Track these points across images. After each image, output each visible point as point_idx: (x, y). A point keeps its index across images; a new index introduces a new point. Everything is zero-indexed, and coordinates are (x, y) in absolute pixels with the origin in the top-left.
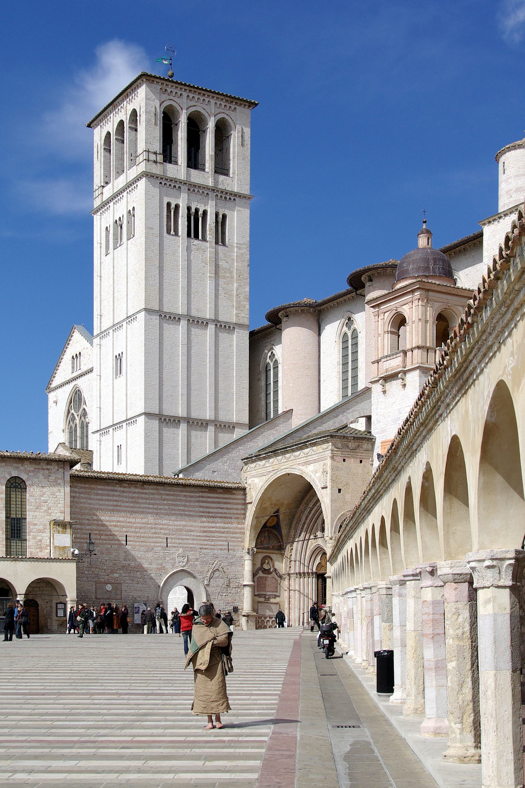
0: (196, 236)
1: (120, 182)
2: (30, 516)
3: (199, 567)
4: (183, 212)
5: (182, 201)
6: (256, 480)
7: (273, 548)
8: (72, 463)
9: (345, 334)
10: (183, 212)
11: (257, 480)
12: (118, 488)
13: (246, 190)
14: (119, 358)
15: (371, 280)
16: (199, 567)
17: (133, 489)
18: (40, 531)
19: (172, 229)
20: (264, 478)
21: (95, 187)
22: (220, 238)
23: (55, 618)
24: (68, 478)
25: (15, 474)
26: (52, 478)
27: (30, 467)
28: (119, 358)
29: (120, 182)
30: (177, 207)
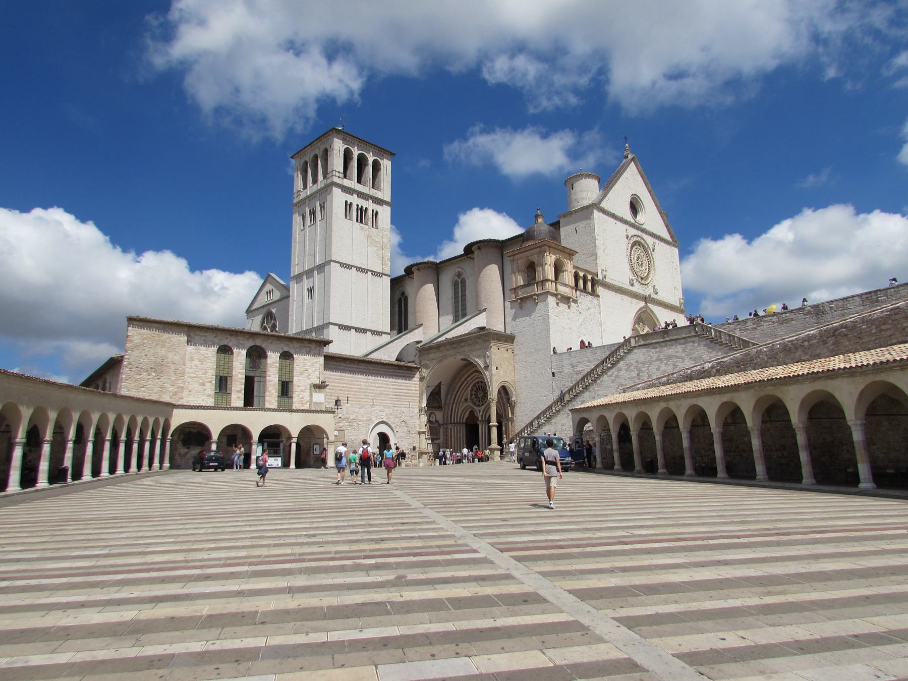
2: (296, 380)
3: (392, 420)
4: (354, 207)
5: (355, 200)
7: (436, 407)
10: (354, 207)
12: (343, 364)
13: (388, 199)
15: (479, 248)
16: (392, 420)
17: (352, 365)
18: (302, 391)
21: (295, 191)
23: (312, 455)
25: (286, 349)
27: (297, 345)
30: (351, 204)
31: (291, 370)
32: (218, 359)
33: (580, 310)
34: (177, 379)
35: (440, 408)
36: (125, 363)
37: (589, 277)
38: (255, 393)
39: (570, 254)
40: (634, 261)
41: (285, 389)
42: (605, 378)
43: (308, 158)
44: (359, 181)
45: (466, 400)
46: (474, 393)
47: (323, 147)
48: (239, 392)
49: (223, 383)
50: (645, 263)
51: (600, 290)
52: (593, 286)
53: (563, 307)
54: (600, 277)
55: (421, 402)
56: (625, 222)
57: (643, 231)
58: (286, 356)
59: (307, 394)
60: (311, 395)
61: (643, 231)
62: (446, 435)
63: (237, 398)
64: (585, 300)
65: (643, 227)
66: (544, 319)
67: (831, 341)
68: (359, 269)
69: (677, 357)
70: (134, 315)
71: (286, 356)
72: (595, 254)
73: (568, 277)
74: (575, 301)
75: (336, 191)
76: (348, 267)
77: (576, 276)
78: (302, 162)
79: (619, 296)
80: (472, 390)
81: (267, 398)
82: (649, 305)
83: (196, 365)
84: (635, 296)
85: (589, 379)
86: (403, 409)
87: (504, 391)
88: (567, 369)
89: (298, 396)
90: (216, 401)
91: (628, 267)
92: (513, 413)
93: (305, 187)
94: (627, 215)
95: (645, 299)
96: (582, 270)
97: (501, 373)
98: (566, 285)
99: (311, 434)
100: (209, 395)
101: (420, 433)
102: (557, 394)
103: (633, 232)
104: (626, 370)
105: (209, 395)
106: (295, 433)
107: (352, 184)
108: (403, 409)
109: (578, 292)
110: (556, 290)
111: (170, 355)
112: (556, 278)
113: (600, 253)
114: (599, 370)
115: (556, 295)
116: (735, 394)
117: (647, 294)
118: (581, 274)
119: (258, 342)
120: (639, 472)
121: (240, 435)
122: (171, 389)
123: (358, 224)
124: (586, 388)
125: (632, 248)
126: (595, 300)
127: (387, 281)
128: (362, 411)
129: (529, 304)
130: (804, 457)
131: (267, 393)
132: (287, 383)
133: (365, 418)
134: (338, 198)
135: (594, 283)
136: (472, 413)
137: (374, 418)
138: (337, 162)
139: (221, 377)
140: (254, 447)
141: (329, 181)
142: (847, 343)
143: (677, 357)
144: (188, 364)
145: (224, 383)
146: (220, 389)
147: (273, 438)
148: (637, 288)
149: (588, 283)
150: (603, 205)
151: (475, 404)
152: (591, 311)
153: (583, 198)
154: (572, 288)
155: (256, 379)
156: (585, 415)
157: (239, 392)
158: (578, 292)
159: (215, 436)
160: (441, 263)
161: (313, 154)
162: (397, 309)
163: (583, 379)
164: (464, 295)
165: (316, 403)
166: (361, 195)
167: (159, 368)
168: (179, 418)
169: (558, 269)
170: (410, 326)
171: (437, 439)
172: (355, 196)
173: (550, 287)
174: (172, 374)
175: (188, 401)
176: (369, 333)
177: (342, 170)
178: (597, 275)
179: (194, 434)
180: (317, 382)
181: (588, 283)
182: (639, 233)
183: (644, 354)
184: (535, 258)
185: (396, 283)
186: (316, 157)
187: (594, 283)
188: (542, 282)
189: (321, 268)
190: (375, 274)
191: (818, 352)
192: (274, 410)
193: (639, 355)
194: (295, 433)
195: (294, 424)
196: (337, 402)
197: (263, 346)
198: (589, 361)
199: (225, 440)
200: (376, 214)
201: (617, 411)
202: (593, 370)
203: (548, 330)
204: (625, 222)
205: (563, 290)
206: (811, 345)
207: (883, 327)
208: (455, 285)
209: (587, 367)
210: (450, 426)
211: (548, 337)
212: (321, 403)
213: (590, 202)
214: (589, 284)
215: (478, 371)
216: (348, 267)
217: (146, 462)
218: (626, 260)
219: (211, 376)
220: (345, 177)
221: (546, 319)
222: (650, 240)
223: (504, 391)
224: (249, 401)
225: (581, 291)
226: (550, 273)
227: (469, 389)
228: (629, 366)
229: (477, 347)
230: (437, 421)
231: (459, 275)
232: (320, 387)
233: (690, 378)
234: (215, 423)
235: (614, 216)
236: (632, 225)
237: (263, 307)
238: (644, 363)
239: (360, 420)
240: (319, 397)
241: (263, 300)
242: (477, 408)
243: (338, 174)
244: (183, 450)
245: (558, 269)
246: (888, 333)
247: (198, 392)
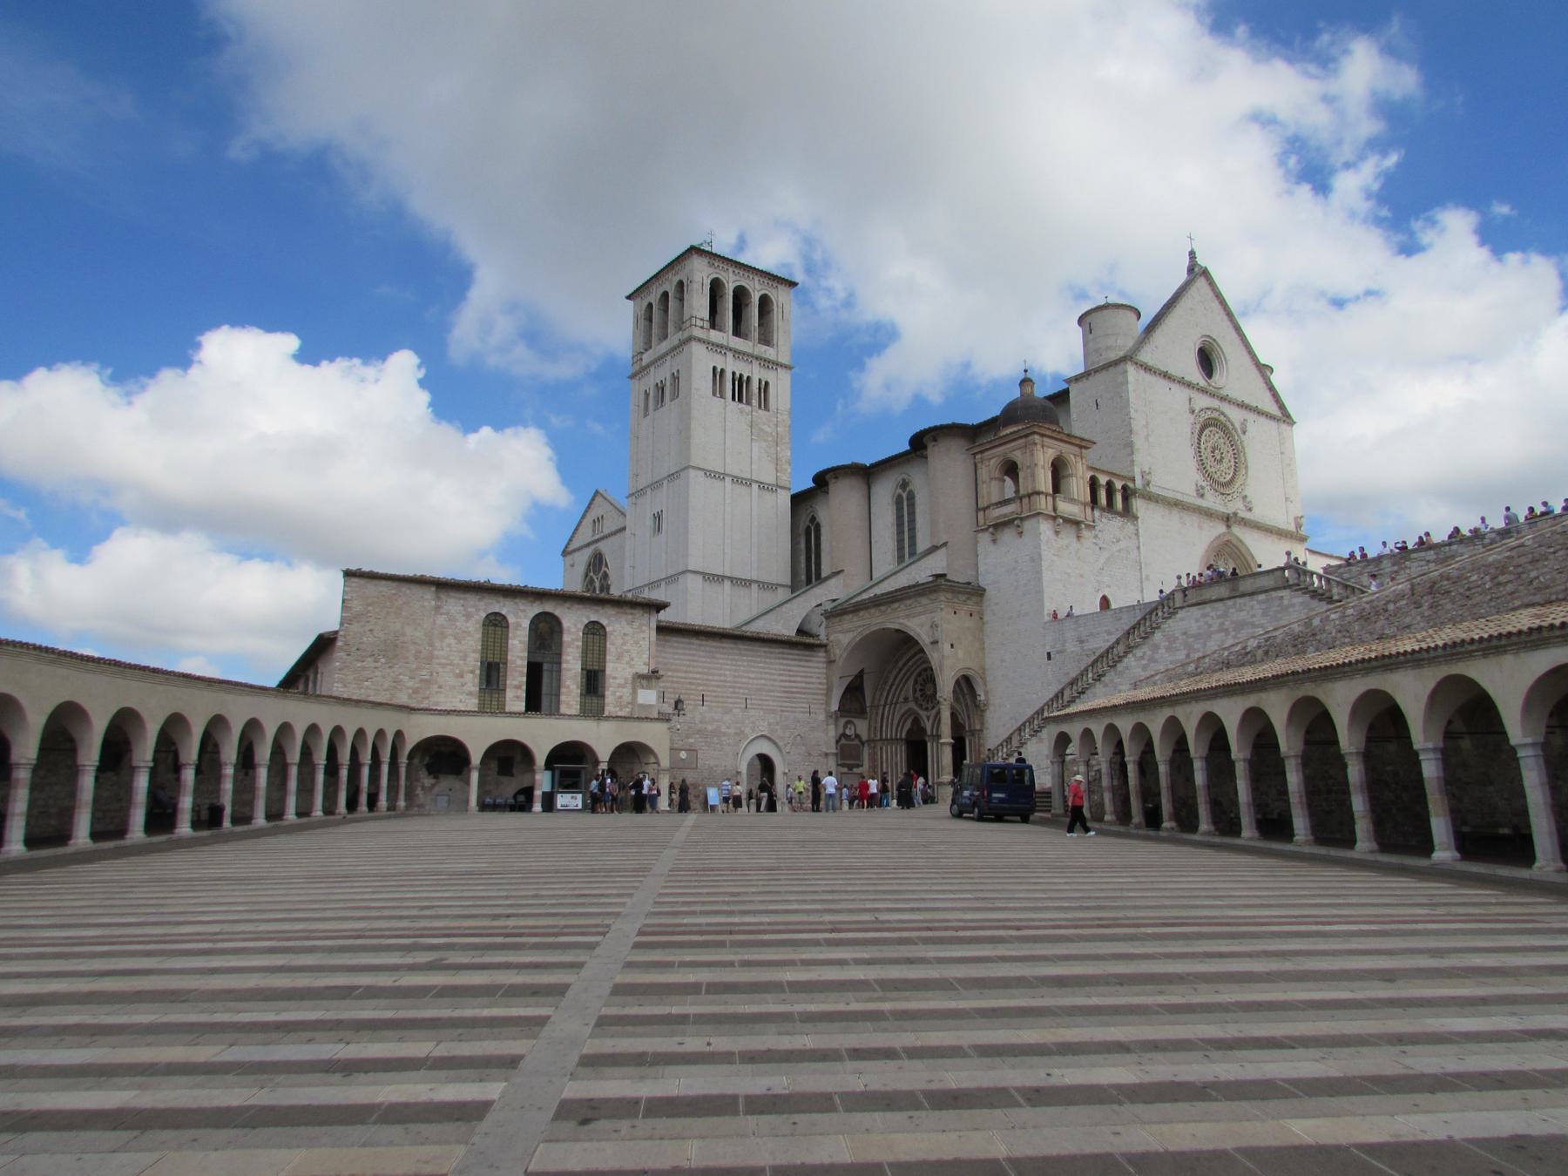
0: (740, 400)
1: (665, 346)
2: (610, 668)
4: (729, 377)
6: (841, 636)
8: (659, 607)
9: (900, 496)
10: (729, 377)
11: (844, 637)
14: (658, 518)
19: (718, 390)
20: (851, 635)
22: (764, 403)
24: (653, 625)
25: (594, 618)
26: (636, 625)
27: (611, 611)
28: (658, 518)
29: (665, 346)
30: (722, 371)
31: (603, 652)
32: (485, 635)
33: (1100, 543)
34: (419, 669)
35: (862, 713)
36: (339, 643)
37: (1118, 485)
38: (545, 689)
39: (1083, 444)
40: (1206, 454)
41: (593, 682)
42: (1130, 660)
43: (654, 297)
44: (737, 332)
45: (906, 700)
46: (918, 687)
47: (676, 280)
48: (518, 687)
49: (492, 674)
50: (1229, 456)
51: (1138, 505)
52: (1126, 499)
53: (1068, 535)
54: (1139, 483)
55: (828, 703)
56: (1189, 385)
57: (1223, 399)
58: (595, 631)
59: (626, 692)
60: (634, 693)
61: (1223, 399)
62: (873, 758)
63: (515, 697)
64: (1110, 526)
65: (1224, 392)
66: (1032, 560)
67: (1426, 602)
68: (737, 480)
69: (1253, 625)
70: (354, 567)
71: (595, 631)
72: (1130, 445)
73: (1078, 486)
74: (1089, 527)
75: (697, 350)
76: (719, 476)
77: (1093, 483)
78: (645, 304)
79: (1176, 516)
80: (916, 682)
81: (563, 698)
82: (1236, 530)
83: (449, 645)
84: (1208, 514)
85: (1107, 660)
86: (799, 716)
87: (965, 685)
88: (1072, 647)
89: (614, 693)
90: (482, 704)
91: (1192, 464)
92: (982, 724)
93: (648, 346)
94: (1195, 374)
95: (1228, 520)
96: (1103, 472)
97: (961, 653)
98: (1072, 501)
99: (630, 753)
100: (470, 694)
101: (826, 755)
102: (1055, 689)
103: (1202, 401)
104: (1168, 649)
105: (470, 694)
106: (604, 754)
107: (725, 337)
108: (799, 716)
109: (1097, 513)
110: (1055, 509)
111: (408, 630)
112: (1056, 488)
113: (1138, 442)
114: (1121, 649)
115: (1054, 518)
116: (1263, 695)
117: (1229, 510)
118: (1103, 480)
119: (549, 607)
120: (1138, 827)
121: (518, 758)
122: (410, 684)
123: (736, 404)
124: (1099, 678)
125: (1202, 431)
126: (1130, 527)
127: (784, 500)
128: (727, 718)
129: (1008, 535)
130: (1359, 803)
131: (563, 690)
132: (596, 672)
133: (731, 731)
134: (701, 362)
135: (1127, 494)
136: (917, 721)
137: (747, 731)
138: (699, 304)
139: (490, 665)
140: (538, 777)
141: (686, 335)
142: (1449, 606)
143: (1253, 625)
144: (438, 644)
145: (494, 674)
146: (488, 682)
147: (570, 761)
148: (1212, 501)
149: (1116, 497)
150: (1145, 356)
151: (921, 706)
152: (1122, 544)
153: (1108, 348)
154: (1085, 505)
155: (545, 666)
156: (1065, 728)
157: (518, 687)
158: (1097, 513)
159: (476, 758)
160: (874, 466)
161: (661, 291)
162: (803, 545)
163: (1096, 661)
164: (912, 521)
165: (642, 706)
166: (738, 354)
167: (391, 651)
168: (419, 729)
169: (1058, 470)
170: (824, 575)
171: (858, 766)
172: (730, 355)
173: (1044, 504)
174: (412, 659)
175: (437, 704)
176: (755, 586)
177: (706, 314)
178: (1133, 480)
179: (444, 756)
180: (644, 670)
181: (1116, 497)
182: (1216, 403)
183: (1197, 620)
184: (1018, 456)
185: (799, 500)
186: (665, 295)
187: (1127, 494)
188: (1029, 496)
189: (672, 477)
190: (763, 486)
191: (1408, 620)
192: (570, 716)
193: (1187, 621)
194: (604, 754)
195: (603, 739)
196: (678, 704)
197: (557, 613)
198: (1109, 633)
199: (494, 765)
200: (765, 387)
201: (1107, 721)
202: (1112, 647)
203: (1040, 580)
204: (1189, 385)
205: (1065, 508)
206: (1399, 609)
207: (1502, 579)
208: (899, 502)
209: (1100, 643)
210: (879, 744)
211: (1040, 592)
212: (650, 706)
213: (1121, 354)
214: (1119, 498)
215: (922, 651)
216: (719, 476)
217: (363, 798)
218: (1189, 453)
219: (474, 661)
220: (713, 325)
221: (1036, 559)
222: (1235, 415)
223: (965, 685)
224: (534, 703)
225: (1103, 510)
226: (1044, 481)
227: (911, 681)
228: (1172, 640)
229: (919, 609)
230: (857, 736)
231: (904, 485)
232: (653, 676)
233: (1227, 665)
234: (478, 736)
235: (1166, 376)
236: (1203, 391)
237: (588, 545)
238: (1197, 636)
239: (724, 734)
240: (648, 696)
241: (586, 535)
242: (923, 714)
243: (700, 323)
244: (428, 781)
245: (1058, 470)
246: (1510, 588)
247: (453, 688)
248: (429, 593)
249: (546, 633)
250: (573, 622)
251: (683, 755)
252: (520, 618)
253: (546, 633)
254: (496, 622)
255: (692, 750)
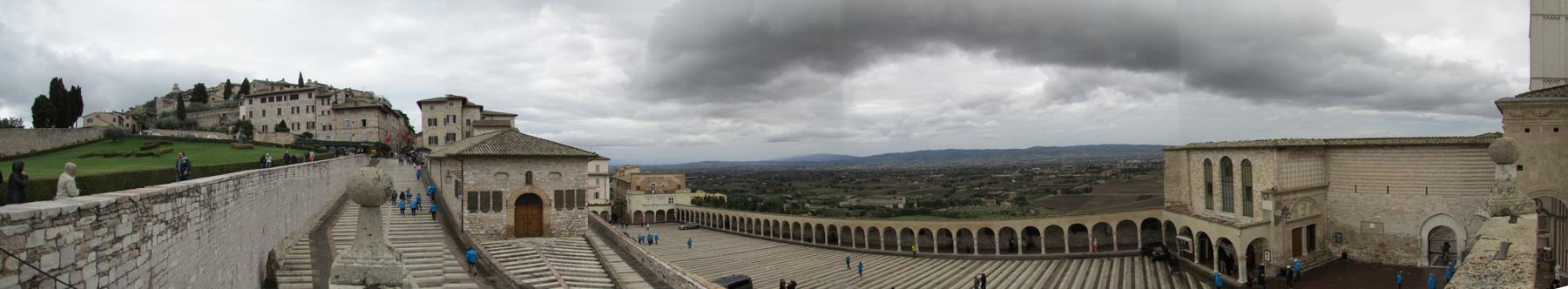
41: (1248, 192)
58: (1246, 164)
71: (1246, 164)
219: (1202, 183)
248: (1184, 153)
249: (1226, 166)
250: (1236, 159)
251: (1372, 226)
252: (1216, 159)
253: (1226, 166)
254: (1208, 163)
255: (1379, 224)
